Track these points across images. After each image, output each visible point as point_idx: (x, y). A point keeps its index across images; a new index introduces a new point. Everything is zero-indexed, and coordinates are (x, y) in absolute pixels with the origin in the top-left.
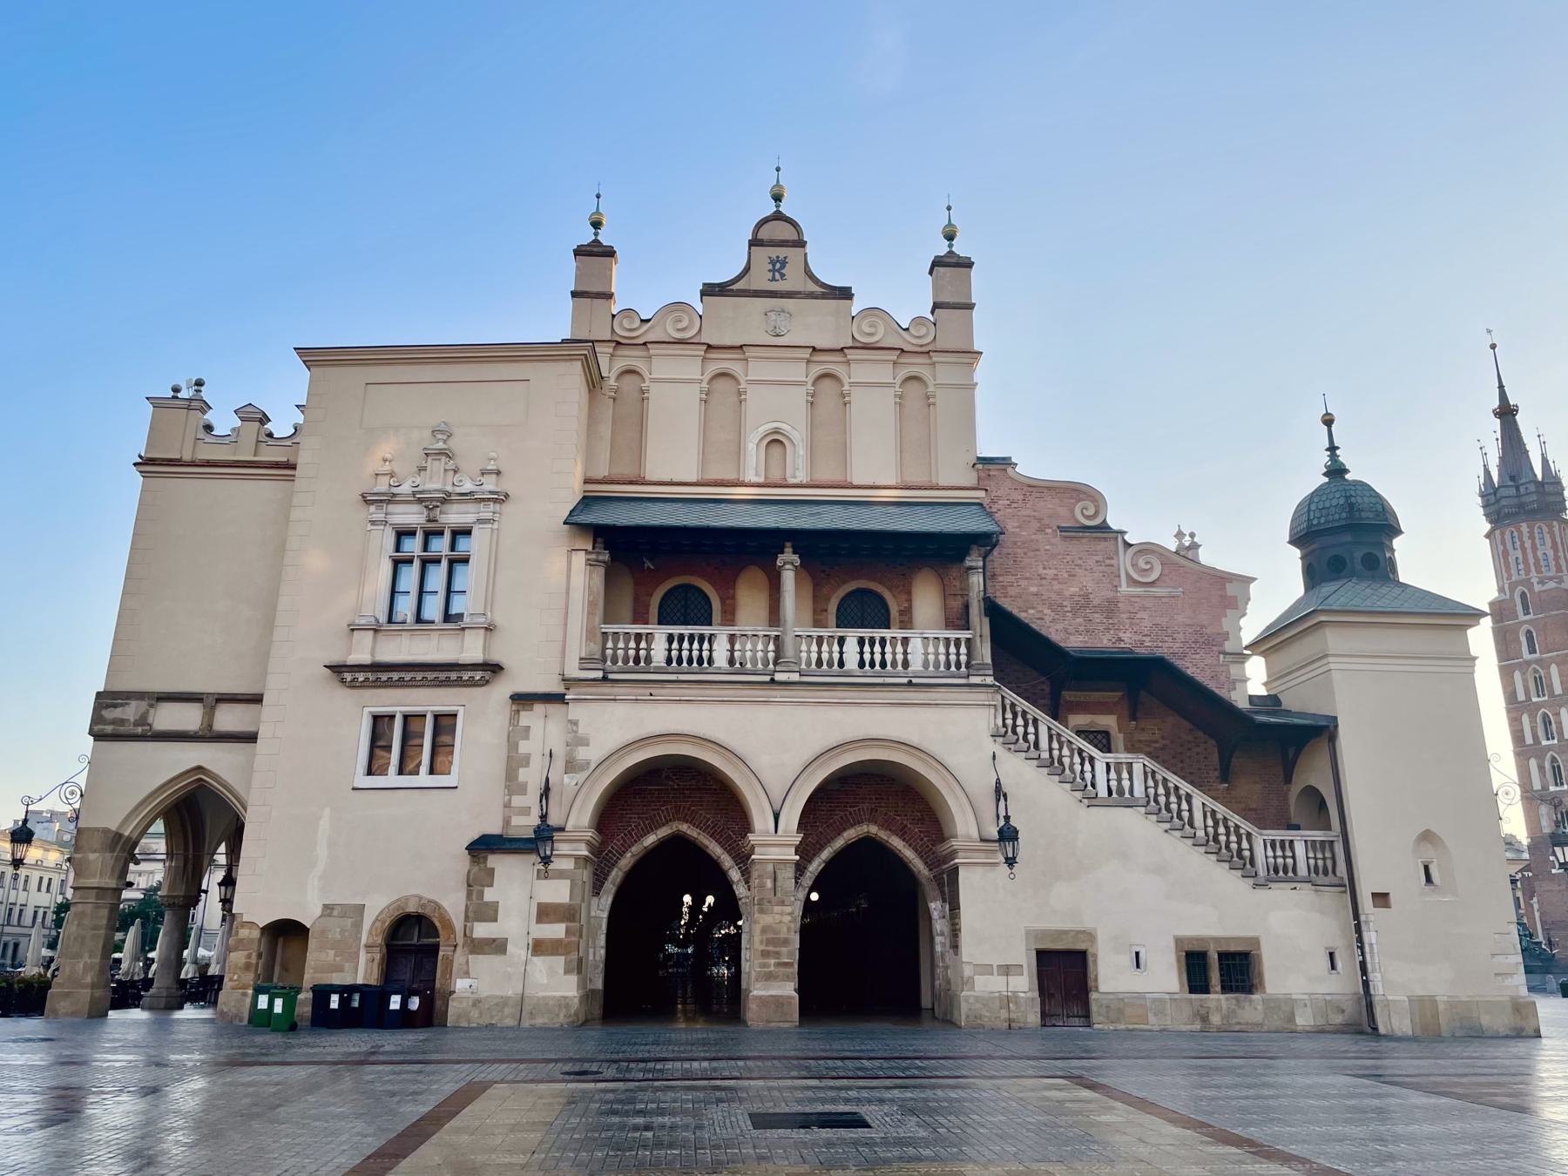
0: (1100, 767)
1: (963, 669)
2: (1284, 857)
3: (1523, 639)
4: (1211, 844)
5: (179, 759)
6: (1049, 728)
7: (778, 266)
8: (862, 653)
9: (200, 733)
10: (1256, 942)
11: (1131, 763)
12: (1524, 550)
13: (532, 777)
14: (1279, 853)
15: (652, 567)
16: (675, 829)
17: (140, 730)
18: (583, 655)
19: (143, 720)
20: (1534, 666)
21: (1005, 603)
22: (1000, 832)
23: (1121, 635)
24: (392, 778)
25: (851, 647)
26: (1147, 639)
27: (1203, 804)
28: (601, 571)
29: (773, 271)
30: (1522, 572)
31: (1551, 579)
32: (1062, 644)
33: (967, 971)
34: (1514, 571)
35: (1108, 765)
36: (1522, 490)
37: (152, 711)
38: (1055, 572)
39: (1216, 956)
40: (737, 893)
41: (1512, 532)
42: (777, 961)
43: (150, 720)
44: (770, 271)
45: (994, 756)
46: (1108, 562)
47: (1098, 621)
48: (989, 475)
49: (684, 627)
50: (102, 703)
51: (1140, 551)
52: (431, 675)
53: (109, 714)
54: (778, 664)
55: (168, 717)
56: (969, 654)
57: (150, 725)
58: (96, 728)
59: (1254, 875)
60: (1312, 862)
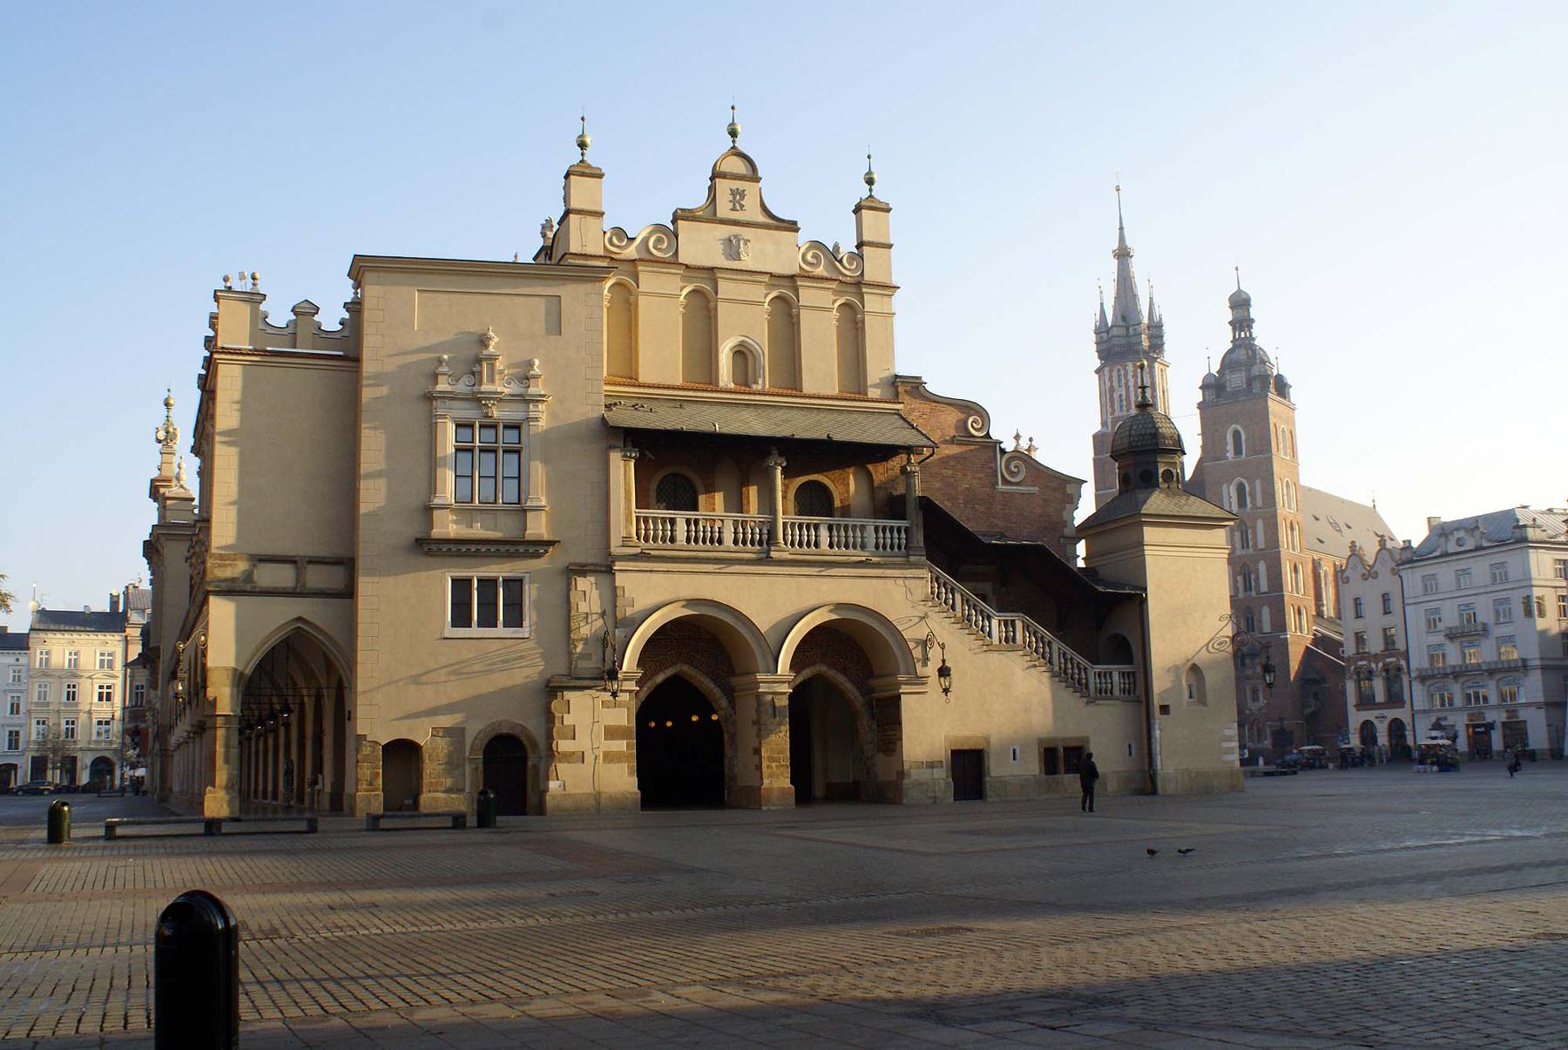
0: (995, 622)
2: (1106, 683)
7: (738, 197)
10: (1086, 740)
12: (1127, 388)
15: (653, 458)
16: (678, 669)
17: (248, 587)
18: (625, 536)
19: (248, 577)
27: (1059, 648)
29: (733, 201)
30: (1125, 409)
33: (906, 767)
34: (1117, 406)
36: (1131, 330)
39: (1062, 750)
41: (1119, 371)
44: (731, 201)
50: (214, 564)
52: (503, 548)
57: (255, 583)
60: (1122, 685)
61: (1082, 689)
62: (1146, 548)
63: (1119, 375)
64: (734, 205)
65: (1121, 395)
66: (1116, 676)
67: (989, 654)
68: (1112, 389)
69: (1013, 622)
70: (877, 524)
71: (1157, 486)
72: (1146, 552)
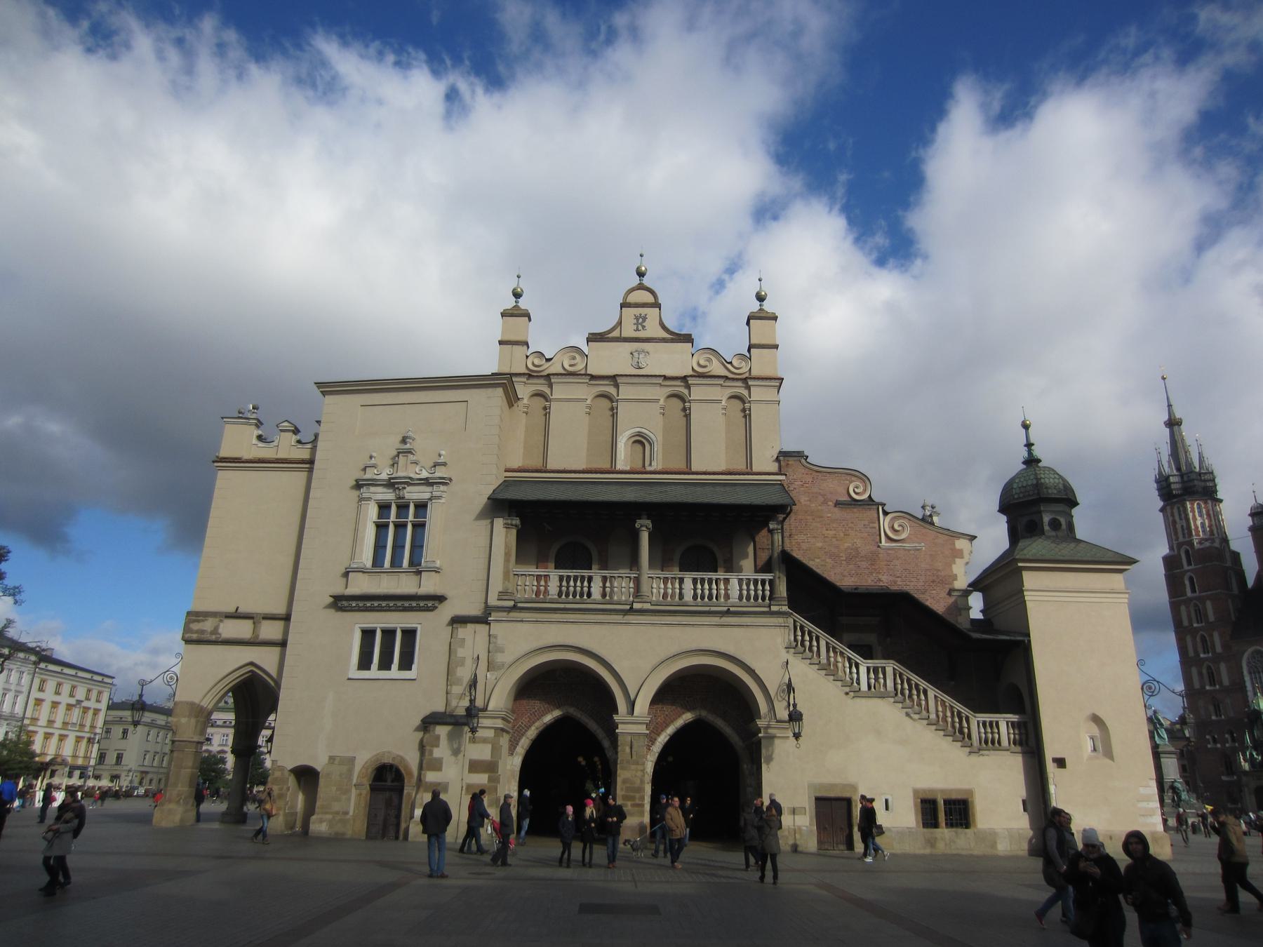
0: (863, 670)
1: (767, 601)
3: (1187, 583)
4: (937, 724)
5: (237, 658)
6: (827, 643)
7: (641, 320)
8: (695, 589)
9: (252, 640)
10: (970, 792)
11: (885, 667)
13: (464, 673)
14: (989, 730)
17: (213, 637)
18: (501, 590)
20: (1195, 601)
21: (797, 554)
22: (790, 715)
23: (880, 577)
24: (374, 672)
25: (688, 584)
26: (899, 579)
27: (935, 696)
28: (514, 532)
29: (637, 324)
31: (1206, 540)
32: (838, 584)
35: (868, 669)
36: (1185, 479)
37: (221, 625)
38: (834, 532)
40: (608, 756)
42: (633, 802)
43: (220, 630)
44: (635, 324)
45: (787, 663)
46: (871, 525)
47: (865, 567)
48: (788, 464)
49: (570, 571)
51: (895, 517)
53: (195, 626)
54: (637, 596)
55: (231, 629)
56: (771, 591)
57: (220, 634)
58: (187, 636)
59: (970, 745)
61: (964, 738)
62: (1025, 593)
63: (1179, 512)
64: (637, 328)
65: (1182, 526)
66: (1003, 727)
67: (858, 700)
68: (1174, 522)
69: (884, 669)
70: (740, 577)
71: (1042, 532)
72: (1026, 598)
